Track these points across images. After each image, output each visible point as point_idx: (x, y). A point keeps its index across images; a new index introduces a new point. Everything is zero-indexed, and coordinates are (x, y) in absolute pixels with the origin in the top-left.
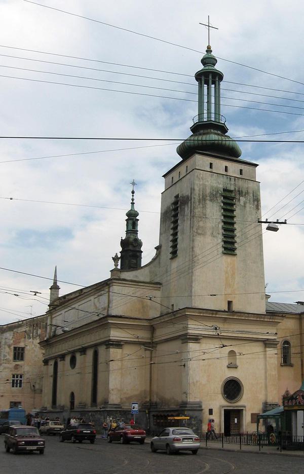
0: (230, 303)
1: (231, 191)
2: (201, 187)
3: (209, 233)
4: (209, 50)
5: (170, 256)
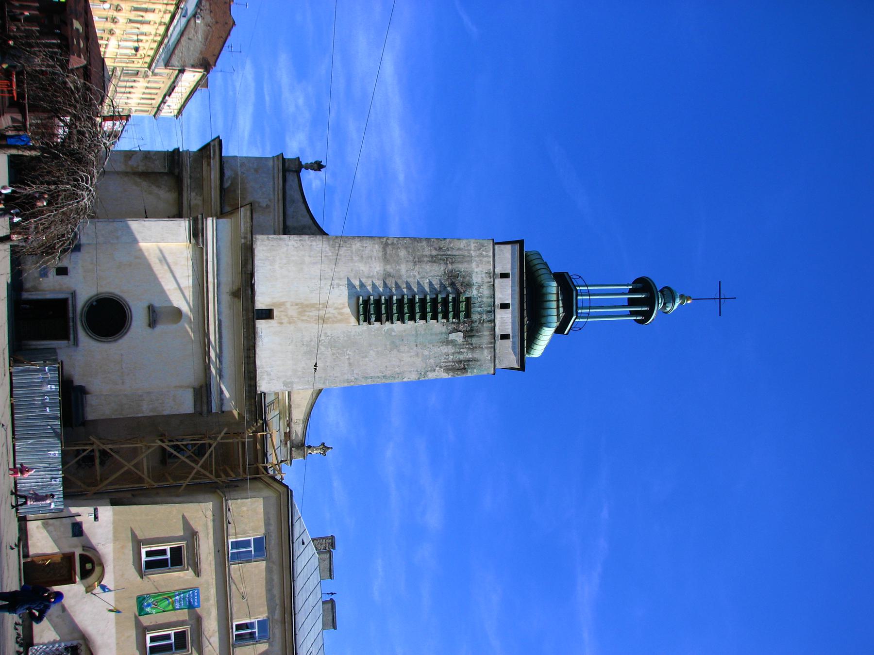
0: (268, 314)
1: (468, 315)
2: (466, 253)
3: (389, 268)
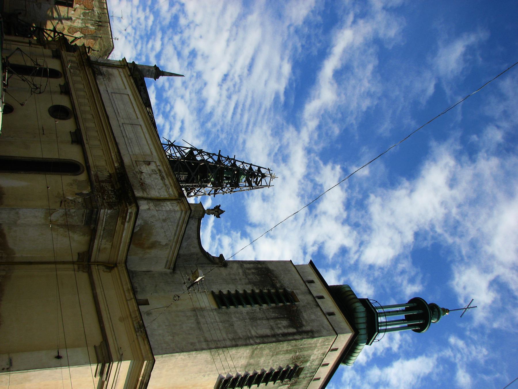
1: (298, 375)
3: (252, 361)
4: (445, 311)
5: (216, 292)
